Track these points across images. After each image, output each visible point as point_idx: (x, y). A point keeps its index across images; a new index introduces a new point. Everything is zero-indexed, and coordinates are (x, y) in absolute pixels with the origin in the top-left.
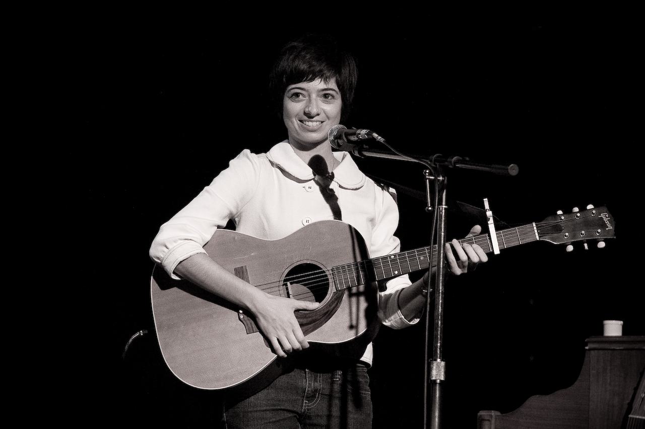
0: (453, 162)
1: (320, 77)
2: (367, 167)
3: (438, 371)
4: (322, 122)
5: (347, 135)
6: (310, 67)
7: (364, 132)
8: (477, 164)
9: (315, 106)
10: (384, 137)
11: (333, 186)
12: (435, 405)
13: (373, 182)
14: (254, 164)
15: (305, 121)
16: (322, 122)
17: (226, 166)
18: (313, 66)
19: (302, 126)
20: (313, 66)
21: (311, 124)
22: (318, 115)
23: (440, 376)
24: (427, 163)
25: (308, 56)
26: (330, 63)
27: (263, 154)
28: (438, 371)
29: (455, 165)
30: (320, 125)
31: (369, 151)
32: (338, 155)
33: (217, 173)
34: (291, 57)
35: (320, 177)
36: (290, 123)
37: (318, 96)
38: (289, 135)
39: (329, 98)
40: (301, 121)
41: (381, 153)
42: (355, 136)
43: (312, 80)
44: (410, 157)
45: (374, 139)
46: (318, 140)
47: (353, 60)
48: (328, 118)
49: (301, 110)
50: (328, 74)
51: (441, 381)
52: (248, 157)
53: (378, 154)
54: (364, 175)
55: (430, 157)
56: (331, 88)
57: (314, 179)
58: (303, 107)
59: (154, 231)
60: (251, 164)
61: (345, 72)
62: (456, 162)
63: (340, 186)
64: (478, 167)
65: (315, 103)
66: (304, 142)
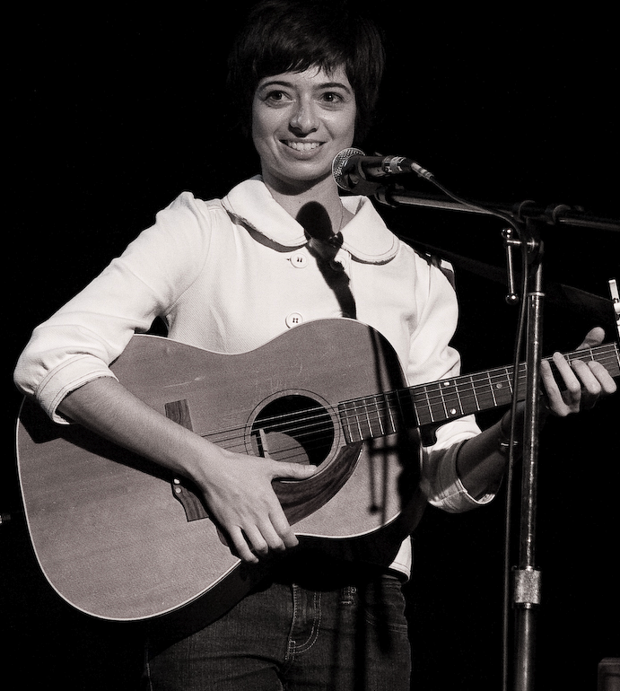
0: (554, 214)
1: (317, 64)
2: (401, 223)
3: (528, 588)
4: (321, 143)
5: (366, 166)
6: (299, 46)
7: (395, 160)
8: (597, 218)
9: (308, 115)
10: (430, 174)
11: (341, 257)
12: (522, 647)
13: (412, 250)
14: (201, 218)
15: (292, 142)
16: (321, 143)
17: (151, 221)
18: (306, 43)
19: (285, 150)
20: (306, 43)
21: (303, 147)
22: (314, 130)
23: (531, 596)
24: (509, 217)
25: (296, 26)
26: (332, 35)
27: (217, 201)
28: (528, 588)
29: (557, 220)
30: (318, 150)
31: (405, 196)
32: (350, 202)
33: (133, 235)
34: (266, 27)
35: (317, 242)
36: (264, 146)
37: (314, 96)
38: (263, 166)
39: (334, 100)
40: (284, 141)
41: (426, 198)
42: (380, 169)
43: (303, 68)
44: (478, 205)
45: (414, 173)
46: (313, 176)
47: (376, 32)
48: (332, 136)
49: (283, 122)
50: (333, 58)
51: (533, 605)
52: (189, 207)
53: (422, 201)
54: (396, 238)
55: (515, 206)
56: (338, 82)
57: (306, 245)
58: (287, 116)
59: (22, 338)
60: (195, 218)
61: (363, 53)
62: (559, 216)
63: (354, 258)
64: (599, 224)
65: (308, 109)
66: (289, 179)
